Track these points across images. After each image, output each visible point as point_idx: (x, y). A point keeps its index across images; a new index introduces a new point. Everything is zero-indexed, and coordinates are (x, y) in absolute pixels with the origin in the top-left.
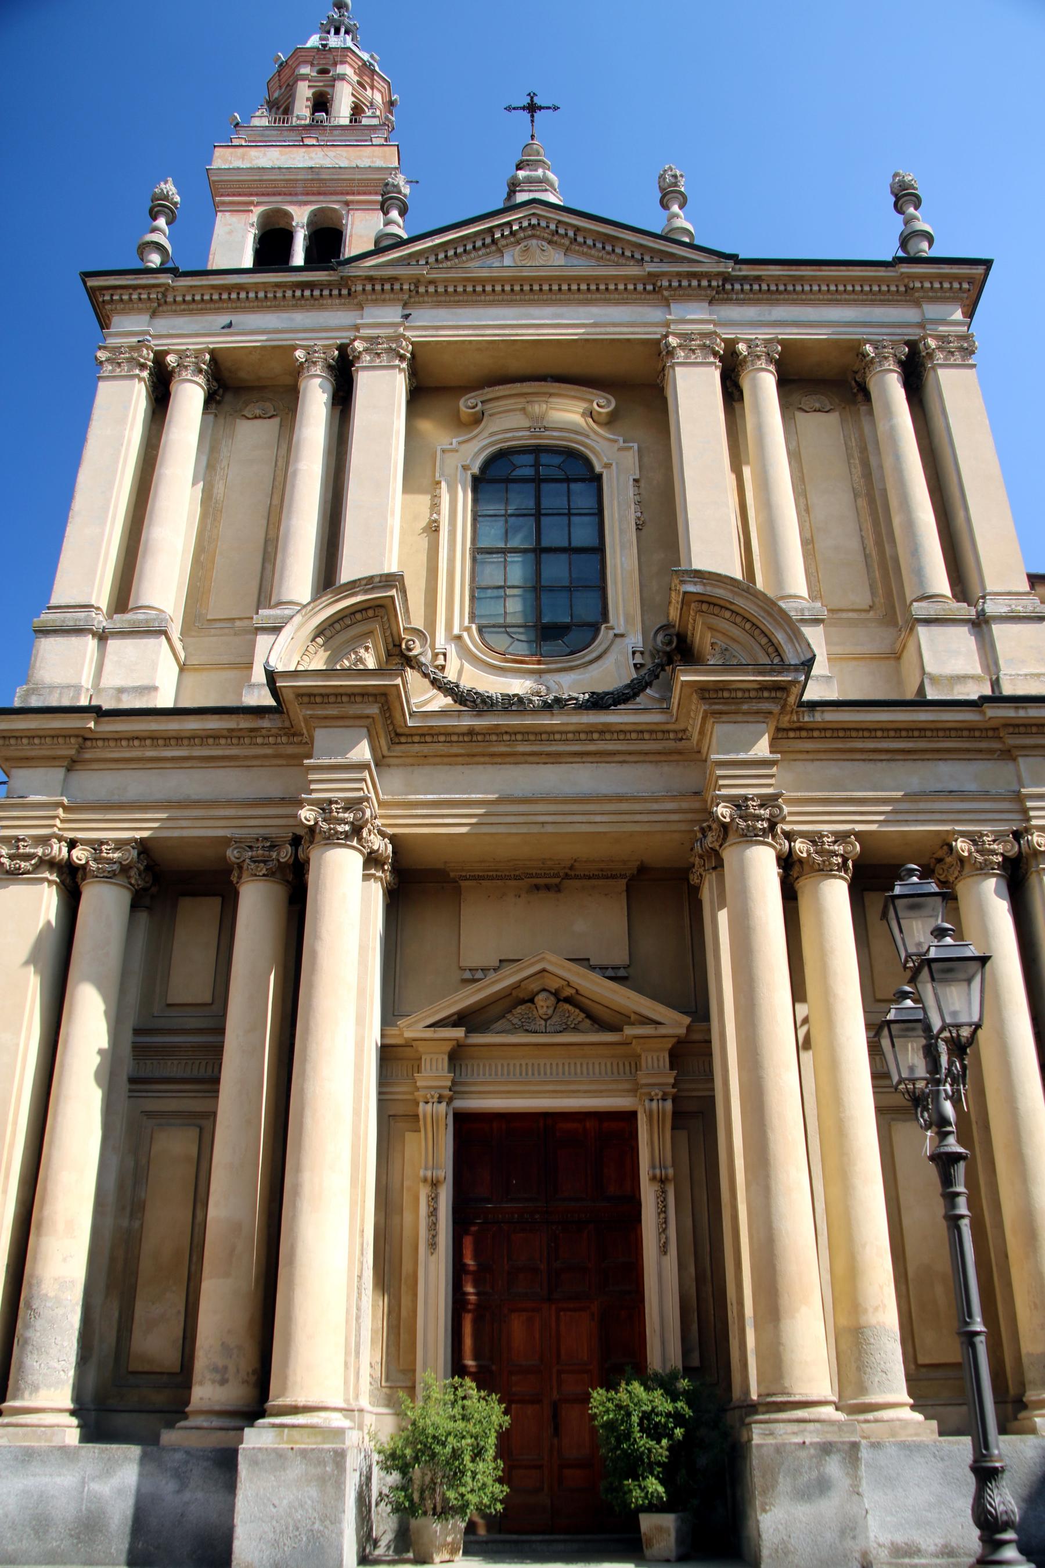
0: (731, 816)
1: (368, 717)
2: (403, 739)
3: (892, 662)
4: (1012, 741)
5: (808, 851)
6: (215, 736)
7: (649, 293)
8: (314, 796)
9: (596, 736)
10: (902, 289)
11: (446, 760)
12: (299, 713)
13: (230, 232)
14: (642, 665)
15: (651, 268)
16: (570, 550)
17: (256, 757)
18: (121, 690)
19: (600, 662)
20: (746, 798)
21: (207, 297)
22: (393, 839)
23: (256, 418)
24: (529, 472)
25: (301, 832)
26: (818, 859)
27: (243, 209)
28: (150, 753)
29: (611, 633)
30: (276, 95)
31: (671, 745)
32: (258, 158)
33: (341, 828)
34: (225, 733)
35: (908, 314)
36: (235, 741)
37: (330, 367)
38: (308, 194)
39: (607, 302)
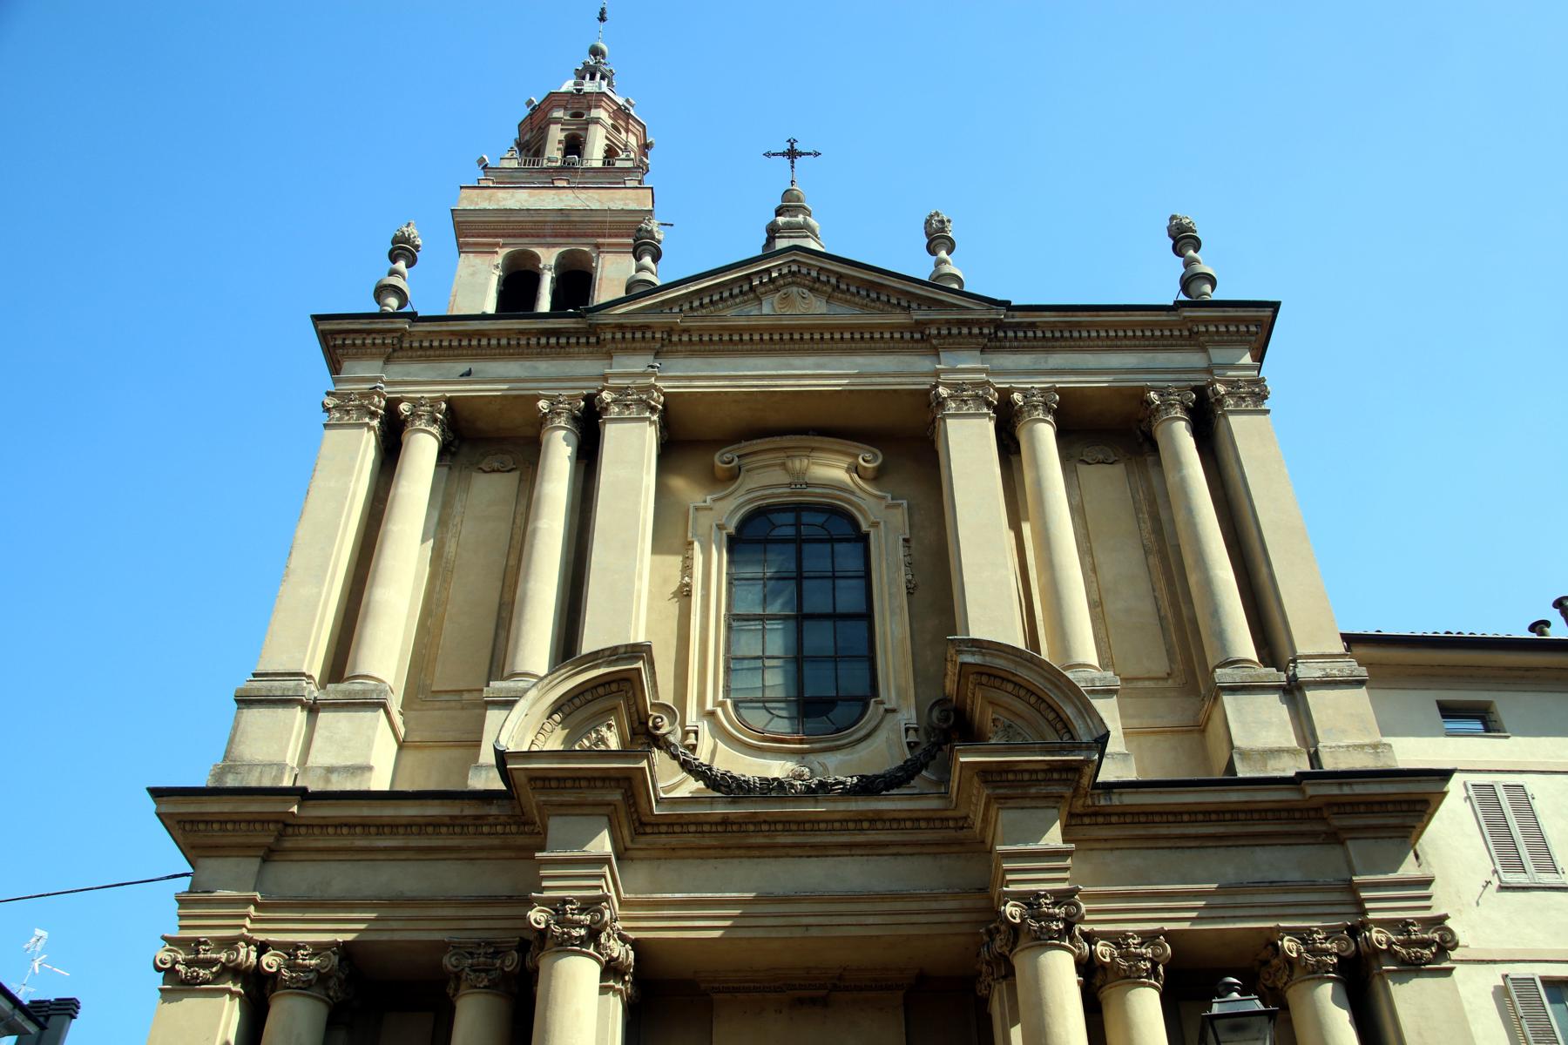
0: (1021, 916)
1: (609, 804)
2: (648, 830)
3: (1196, 735)
4: (1336, 822)
5: (1111, 955)
6: (434, 825)
7: (917, 341)
8: (547, 894)
9: (866, 825)
10: (1186, 333)
11: (696, 853)
12: (532, 799)
13: (473, 274)
14: (917, 744)
15: (918, 315)
16: (834, 617)
17: (481, 849)
18: (330, 770)
19: (869, 741)
20: (1037, 895)
21: (445, 343)
22: (636, 945)
23: (493, 471)
24: (789, 531)
25: (531, 937)
26: (1124, 964)
27: (489, 250)
29: (881, 708)
30: (527, 137)
31: (952, 834)
33: (575, 933)
34: (447, 820)
35: (1195, 359)
36: (457, 830)
39: (872, 351)
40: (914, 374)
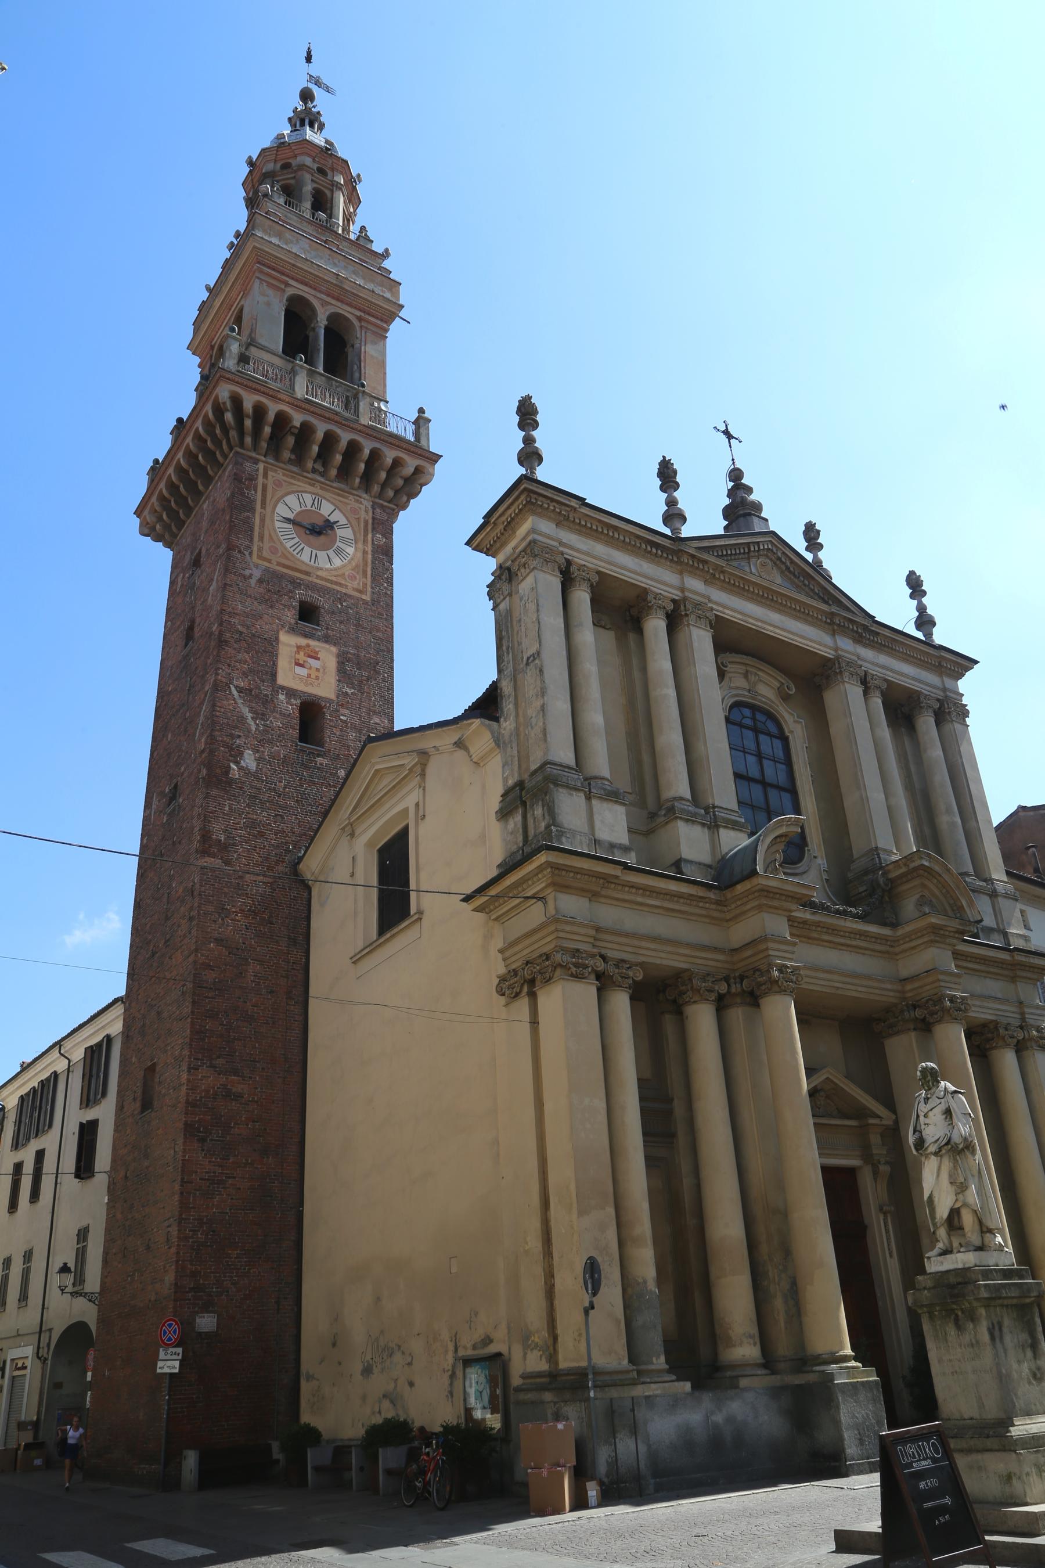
6: (679, 896)
13: (268, 304)
21: (594, 527)
28: (639, 899)
32: (292, 242)
37: (667, 614)
38: (328, 295)
39: (806, 621)
40: (819, 644)
